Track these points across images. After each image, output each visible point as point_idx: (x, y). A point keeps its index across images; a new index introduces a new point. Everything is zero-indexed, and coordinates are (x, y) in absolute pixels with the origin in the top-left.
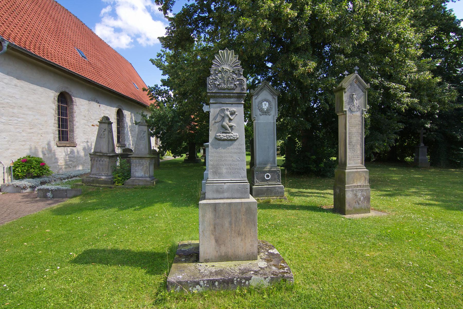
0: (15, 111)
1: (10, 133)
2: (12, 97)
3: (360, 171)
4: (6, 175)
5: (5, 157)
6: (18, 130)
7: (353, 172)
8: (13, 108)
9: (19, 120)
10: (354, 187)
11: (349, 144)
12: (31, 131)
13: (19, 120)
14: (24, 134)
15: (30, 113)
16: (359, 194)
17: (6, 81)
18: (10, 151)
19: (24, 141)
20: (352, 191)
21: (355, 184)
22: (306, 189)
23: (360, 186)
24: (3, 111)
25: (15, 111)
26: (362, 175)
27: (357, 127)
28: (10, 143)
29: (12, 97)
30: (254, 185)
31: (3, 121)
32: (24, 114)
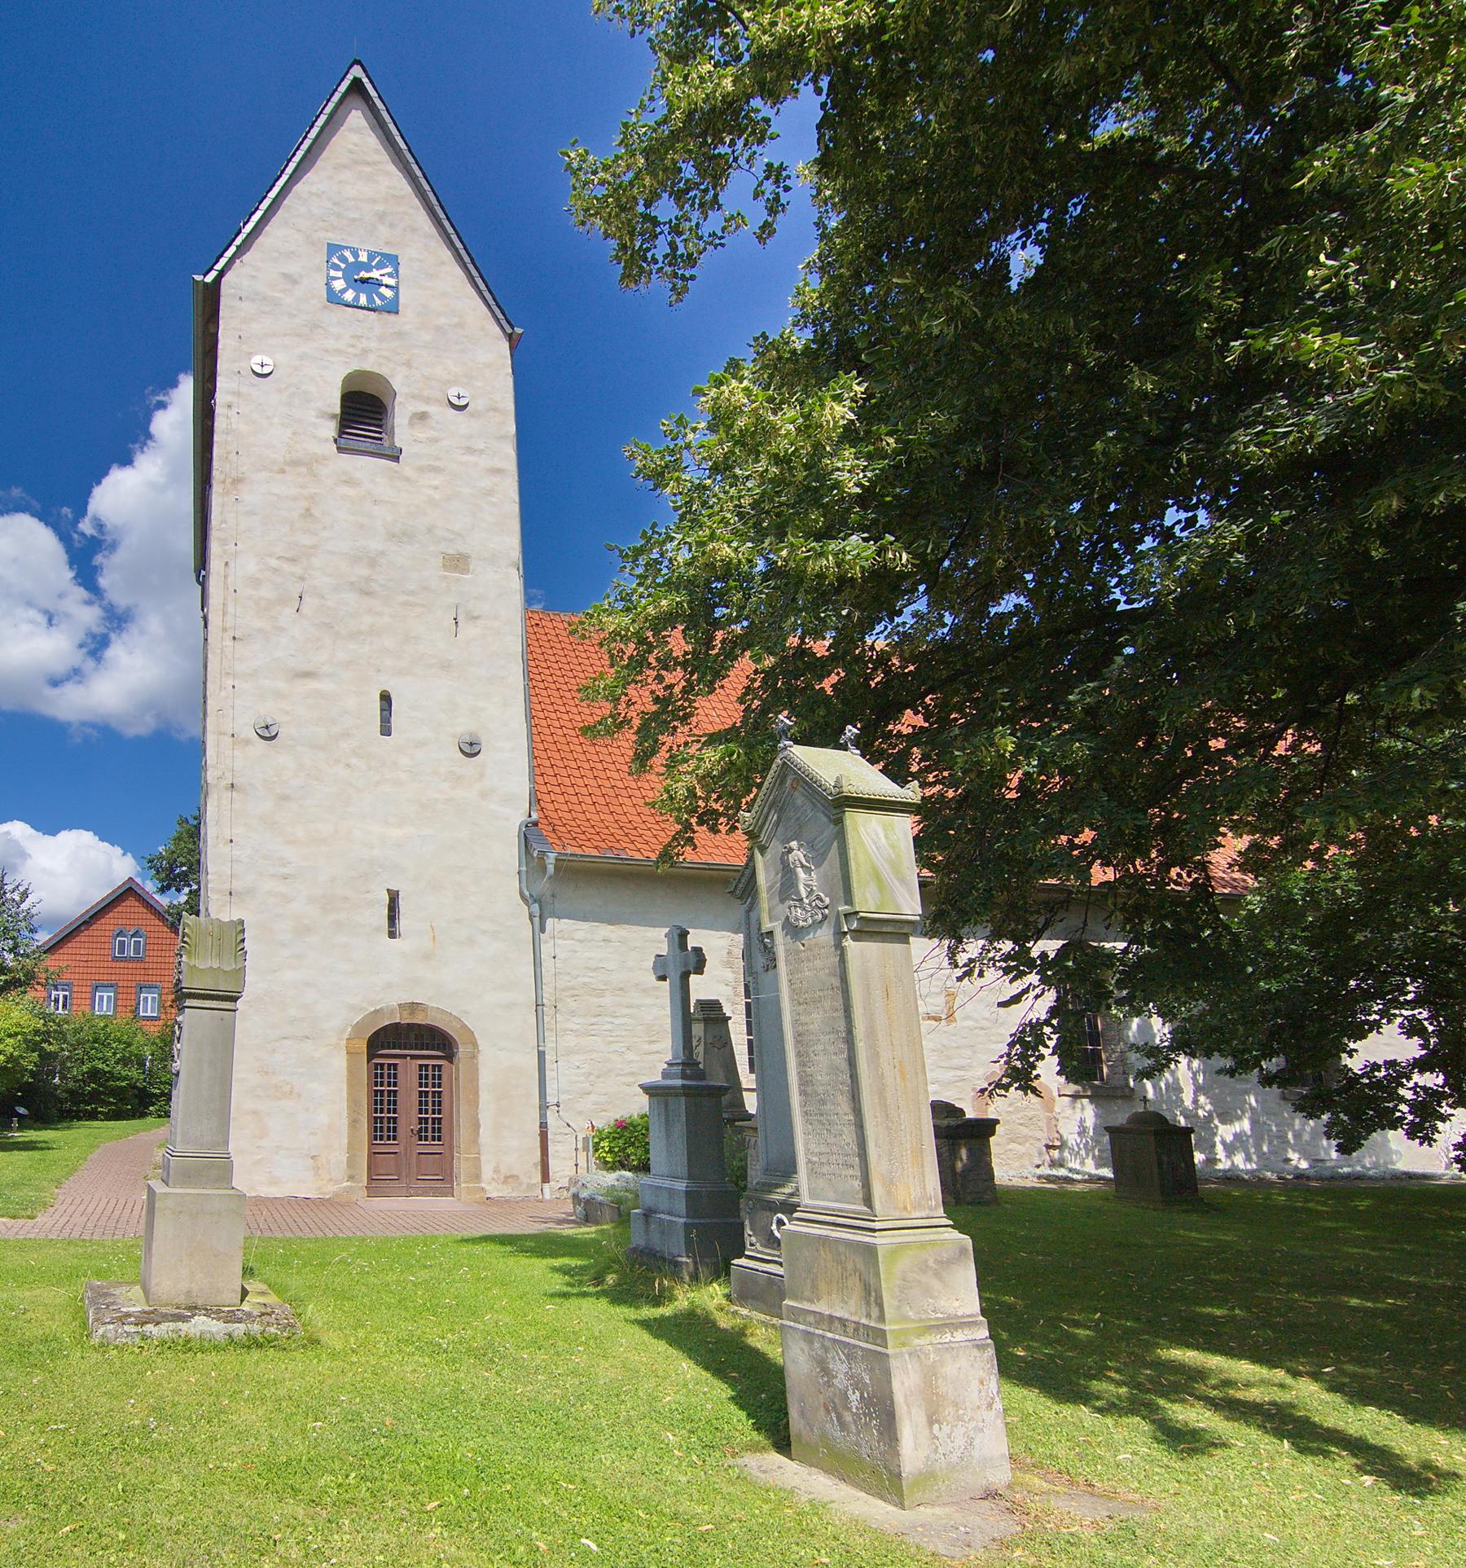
0: (607, 1000)
1: (594, 1056)
2: (595, 970)
3: (838, 1240)
4: (582, 1156)
5: (580, 1113)
6: (614, 1047)
7: (807, 1236)
8: (600, 993)
9: (617, 1022)
10: (817, 1324)
11: (803, 1093)
12: (654, 1047)
13: (617, 1022)
14: (631, 1056)
15: (649, 1001)
16: (839, 1367)
17: (579, 935)
18: (593, 1097)
19: (632, 1074)
20: (808, 1337)
21: (822, 1307)
22: (1362, 1394)
23: (843, 1322)
24: (574, 1004)
25: (607, 1000)
26: (850, 1266)
27: (827, 1004)
28: (592, 1078)
29: (595, 970)
30: (741, 1255)
31: (575, 1027)
32: (629, 1006)
